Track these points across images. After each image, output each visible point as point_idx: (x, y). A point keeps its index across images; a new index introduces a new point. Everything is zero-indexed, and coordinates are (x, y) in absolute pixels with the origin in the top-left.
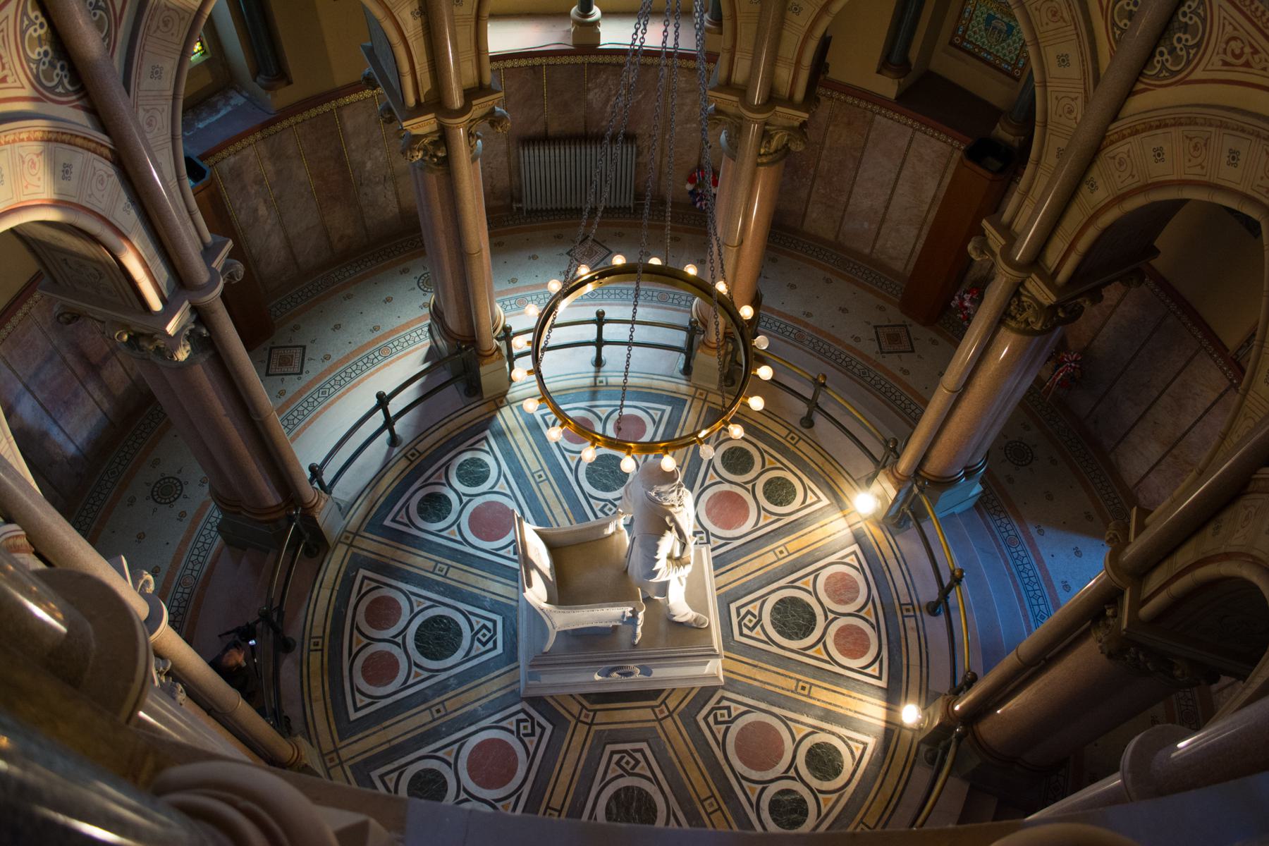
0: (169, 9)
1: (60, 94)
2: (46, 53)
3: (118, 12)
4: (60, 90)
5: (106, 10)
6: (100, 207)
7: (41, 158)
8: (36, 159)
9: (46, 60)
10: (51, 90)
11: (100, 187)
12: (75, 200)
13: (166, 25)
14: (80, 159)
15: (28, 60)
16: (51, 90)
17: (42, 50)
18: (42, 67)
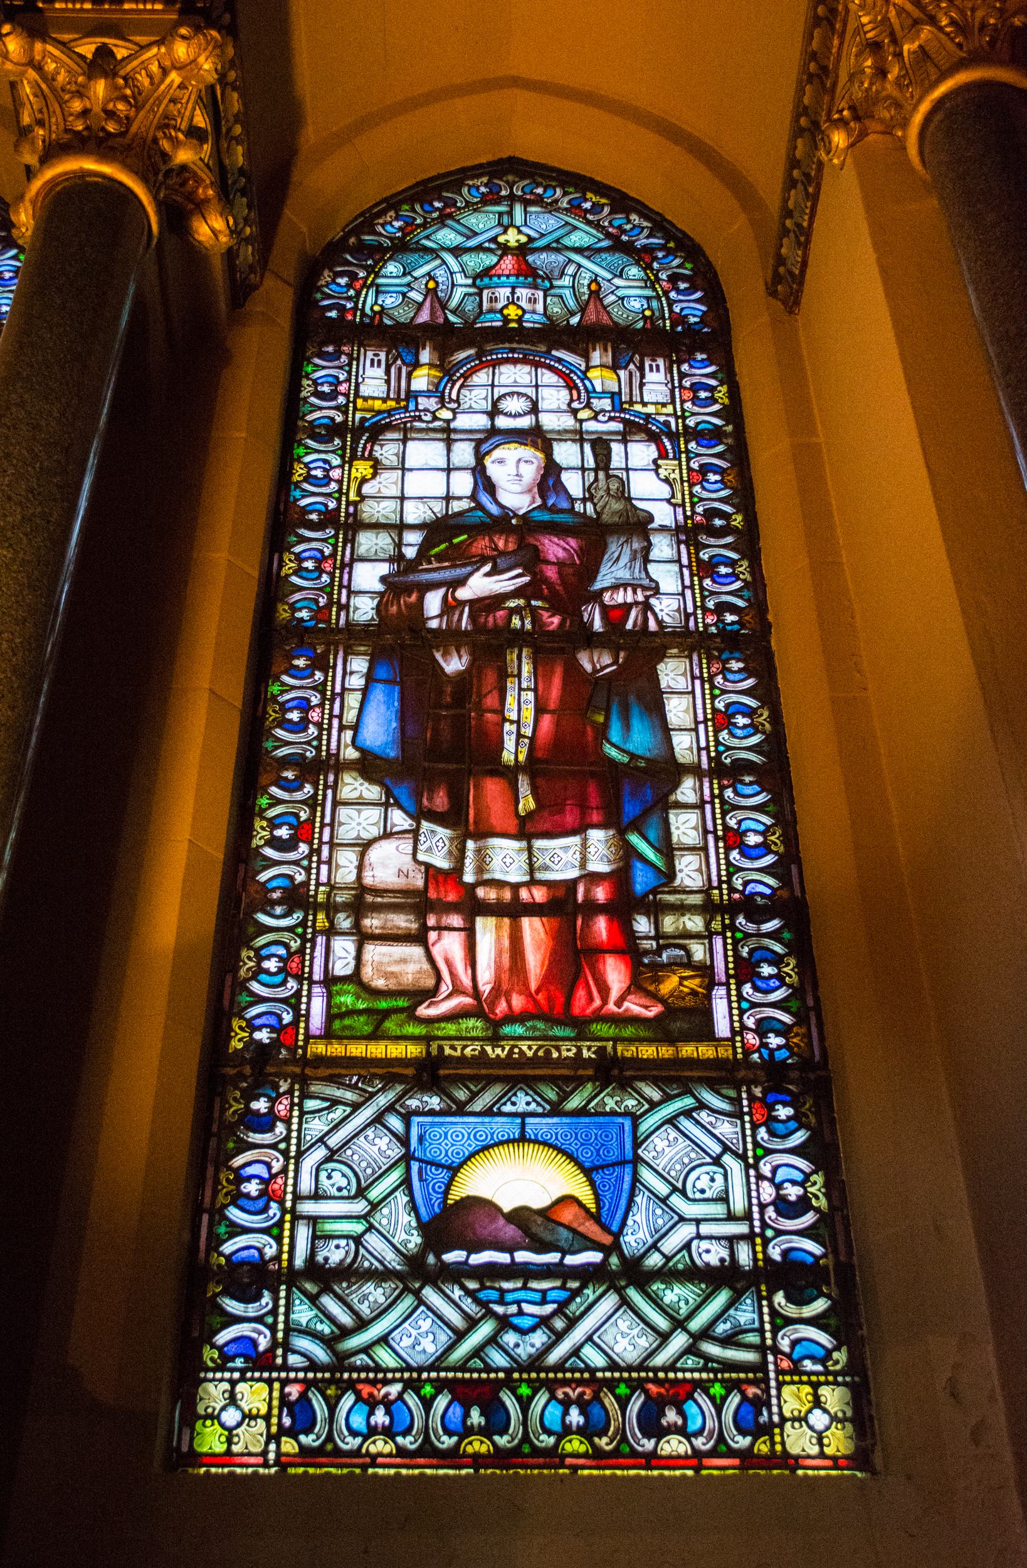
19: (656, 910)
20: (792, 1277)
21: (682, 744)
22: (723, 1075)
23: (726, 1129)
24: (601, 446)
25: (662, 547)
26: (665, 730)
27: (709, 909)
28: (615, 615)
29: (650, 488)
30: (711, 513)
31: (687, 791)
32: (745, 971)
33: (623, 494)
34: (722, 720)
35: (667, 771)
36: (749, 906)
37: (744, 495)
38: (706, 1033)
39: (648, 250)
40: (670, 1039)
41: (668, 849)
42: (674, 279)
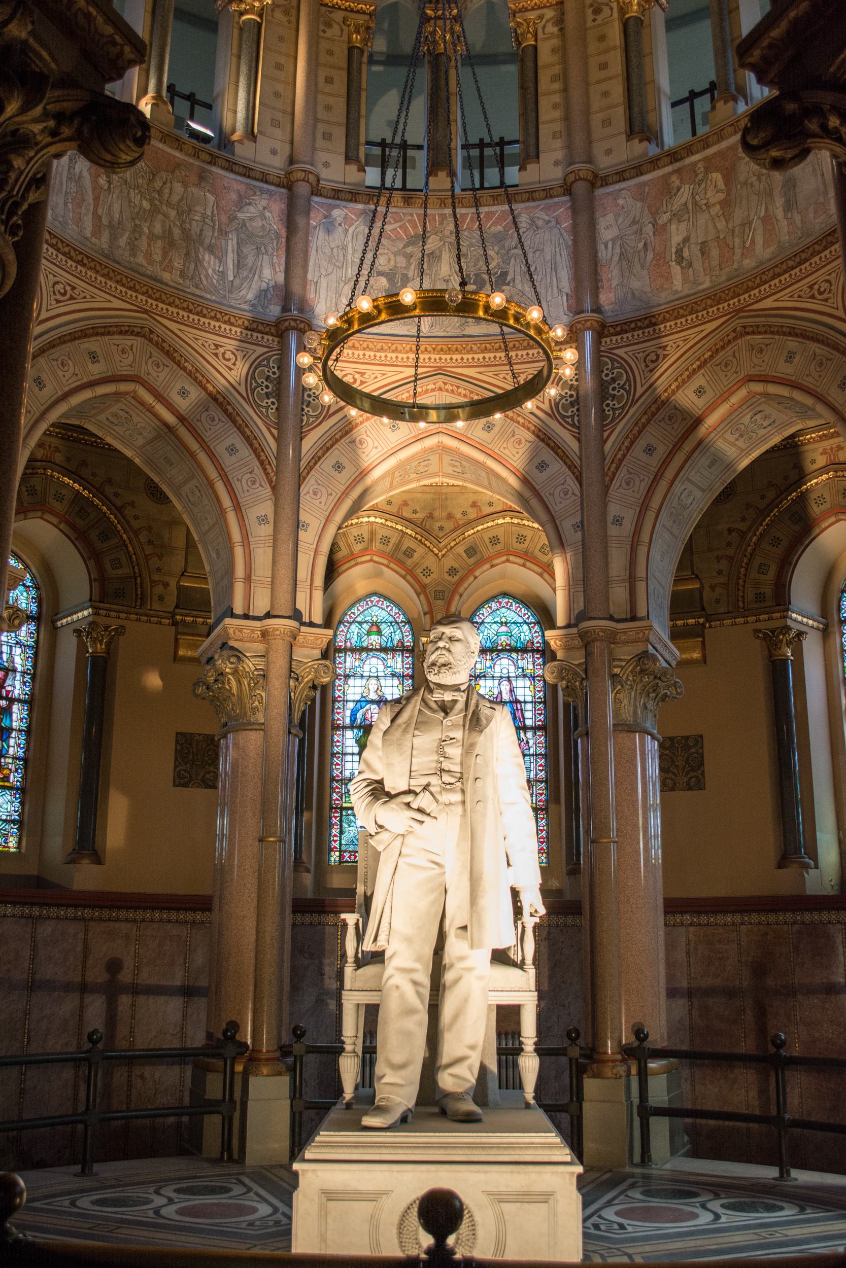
0: (676, 409)
1: (567, 423)
2: (571, 396)
3: (636, 397)
4: (569, 420)
5: (628, 392)
6: (556, 508)
7: (528, 445)
8: (523, 441)
9: (570, 400)
10: (563, 417)
11: (562, 495)
12: (537, 487)
14: (556, 467)
16: (563, 417)
17: (569, 393)
18: (564, 401)
19: (5, 757)
20: (14, 822)
21: (15, 725)
22: (10, 788)
23: (9, 798)
24: (11, 647)
25: (18, 675)
26: (12, 721)
27: (13, 758)
28: (8, 692)
29: (18, 661)
30: (28, 669)
31: (13, 735)
32: (16, 771)
33: (13, 662)
34: (21, 720)
35: (10, 730)
36: (19, 759)
37: (35, 666)
38: (8, 781)
39: (29, 587)
40: (4, 781)
41: (9, 746)
42: (33, 598)
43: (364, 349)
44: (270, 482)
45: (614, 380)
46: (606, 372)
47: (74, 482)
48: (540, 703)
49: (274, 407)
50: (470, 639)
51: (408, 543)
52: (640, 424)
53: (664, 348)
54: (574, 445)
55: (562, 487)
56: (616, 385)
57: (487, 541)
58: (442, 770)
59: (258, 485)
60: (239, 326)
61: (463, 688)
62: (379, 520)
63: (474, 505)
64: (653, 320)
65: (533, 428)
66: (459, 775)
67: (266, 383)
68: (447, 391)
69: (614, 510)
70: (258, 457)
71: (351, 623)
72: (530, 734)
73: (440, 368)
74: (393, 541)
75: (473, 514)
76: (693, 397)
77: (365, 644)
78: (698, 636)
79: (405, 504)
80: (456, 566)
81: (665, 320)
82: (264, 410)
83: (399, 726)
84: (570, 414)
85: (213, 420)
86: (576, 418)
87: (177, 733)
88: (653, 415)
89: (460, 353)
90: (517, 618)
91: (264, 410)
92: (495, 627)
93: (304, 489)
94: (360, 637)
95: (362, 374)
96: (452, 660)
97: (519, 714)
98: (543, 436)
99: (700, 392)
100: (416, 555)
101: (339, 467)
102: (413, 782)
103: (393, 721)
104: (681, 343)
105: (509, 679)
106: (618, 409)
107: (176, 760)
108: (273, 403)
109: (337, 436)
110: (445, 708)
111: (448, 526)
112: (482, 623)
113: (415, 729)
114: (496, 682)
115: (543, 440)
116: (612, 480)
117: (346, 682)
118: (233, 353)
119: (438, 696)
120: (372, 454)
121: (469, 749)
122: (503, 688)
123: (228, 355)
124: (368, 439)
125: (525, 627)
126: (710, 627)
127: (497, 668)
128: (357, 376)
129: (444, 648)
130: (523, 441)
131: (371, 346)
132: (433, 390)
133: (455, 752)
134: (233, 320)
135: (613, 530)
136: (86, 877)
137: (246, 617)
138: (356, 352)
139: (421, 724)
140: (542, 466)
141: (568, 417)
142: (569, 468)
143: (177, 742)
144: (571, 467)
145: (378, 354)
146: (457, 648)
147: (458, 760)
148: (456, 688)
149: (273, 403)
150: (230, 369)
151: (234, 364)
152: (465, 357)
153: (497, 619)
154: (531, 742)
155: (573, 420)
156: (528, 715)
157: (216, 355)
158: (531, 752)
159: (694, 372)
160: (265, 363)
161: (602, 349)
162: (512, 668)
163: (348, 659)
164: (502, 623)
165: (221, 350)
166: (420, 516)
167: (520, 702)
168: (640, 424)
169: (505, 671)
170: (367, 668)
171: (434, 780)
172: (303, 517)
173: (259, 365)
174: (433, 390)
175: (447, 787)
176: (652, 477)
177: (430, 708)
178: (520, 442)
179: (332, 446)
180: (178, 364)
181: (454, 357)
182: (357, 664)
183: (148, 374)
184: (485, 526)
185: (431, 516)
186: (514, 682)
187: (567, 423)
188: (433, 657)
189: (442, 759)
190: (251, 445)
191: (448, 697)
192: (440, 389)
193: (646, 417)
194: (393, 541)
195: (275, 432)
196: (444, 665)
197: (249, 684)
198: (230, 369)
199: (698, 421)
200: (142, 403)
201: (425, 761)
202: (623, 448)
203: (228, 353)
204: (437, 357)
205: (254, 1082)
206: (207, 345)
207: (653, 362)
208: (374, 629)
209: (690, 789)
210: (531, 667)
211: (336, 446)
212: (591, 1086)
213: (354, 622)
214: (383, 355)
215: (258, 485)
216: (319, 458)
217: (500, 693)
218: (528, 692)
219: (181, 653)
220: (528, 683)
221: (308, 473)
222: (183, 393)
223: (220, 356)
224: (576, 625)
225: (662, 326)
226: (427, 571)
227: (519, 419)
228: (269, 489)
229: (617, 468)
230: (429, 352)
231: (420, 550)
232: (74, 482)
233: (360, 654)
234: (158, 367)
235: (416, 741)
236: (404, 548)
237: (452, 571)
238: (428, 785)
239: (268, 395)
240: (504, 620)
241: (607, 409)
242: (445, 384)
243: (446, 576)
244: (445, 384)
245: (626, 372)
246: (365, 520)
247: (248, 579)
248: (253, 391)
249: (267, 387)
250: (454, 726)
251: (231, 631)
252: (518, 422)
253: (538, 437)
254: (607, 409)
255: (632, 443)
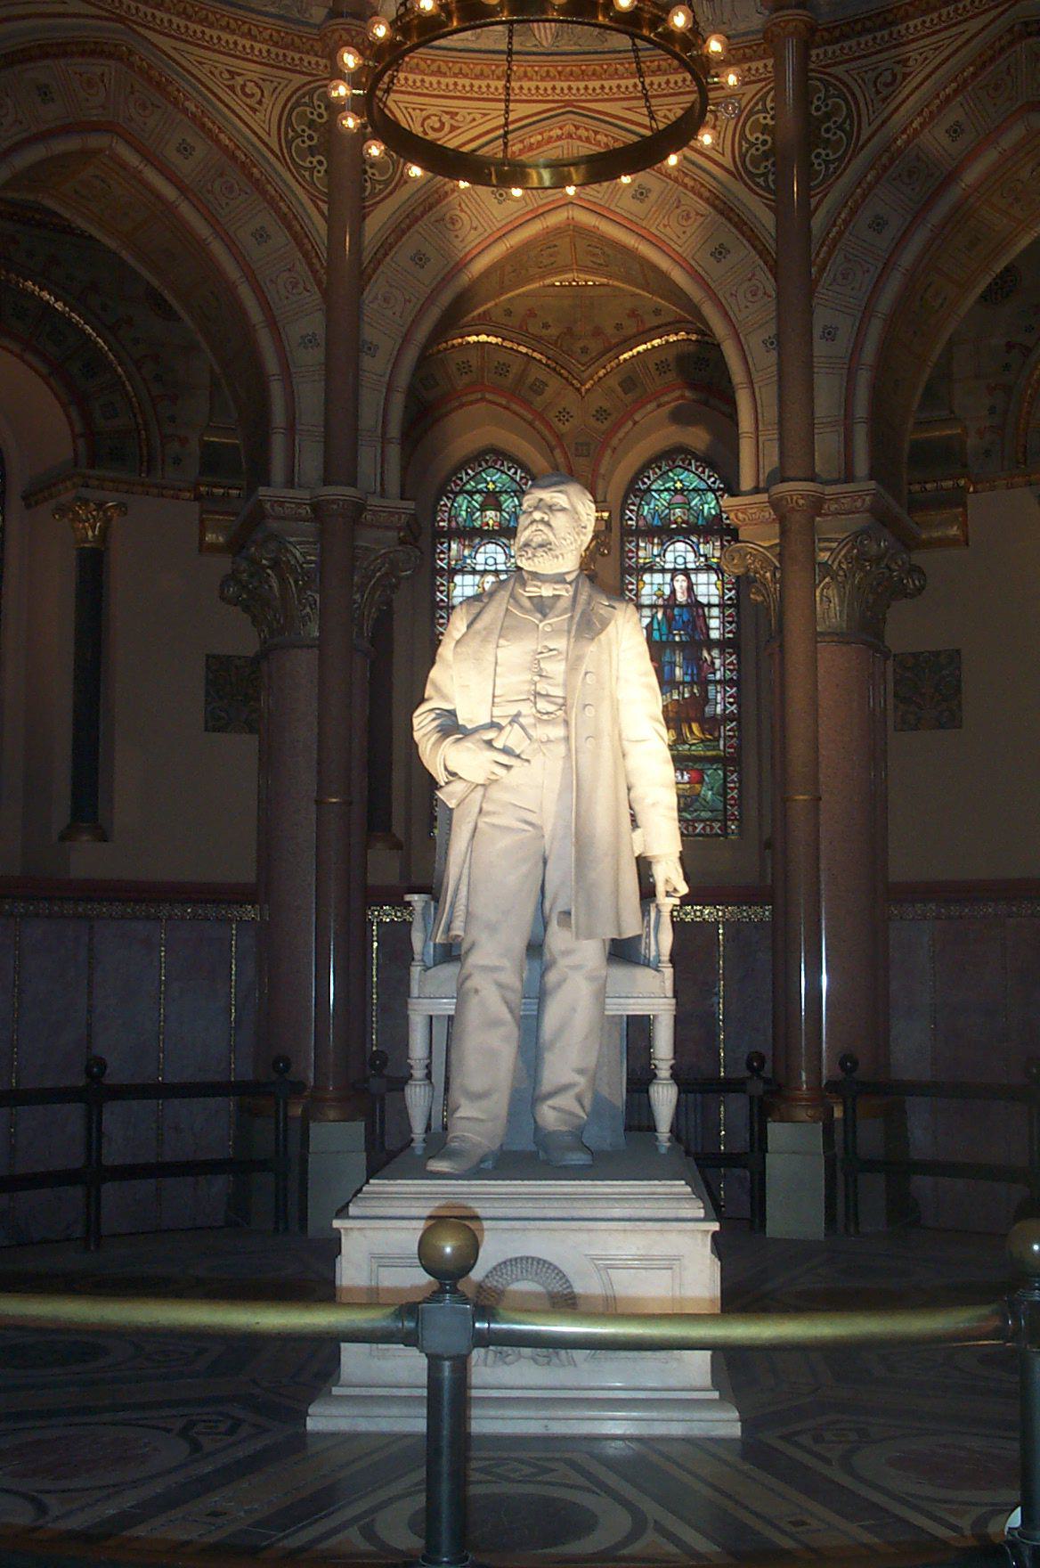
1: (758, 184)
2: (765, 142)
4: (761, 181)
5: (849, 135)
8: (693, 214)
13: (910, 176)
14: (743, 253)
15: (743, 136)
17: (762, 138)
18: (753, 150)
43: (455, 75)
44: (319, 283)
45: (828, 116)
46: (816, 103)
47: (41, 289)
48: (730, 606)
49: (322, 169)
50: (580, 508)
51: (536, 373)
52: (864, 185)
53: (904, 62)
54: (767, 219)
55: (746, 285)
56: (830, 124)
57: (652, 367)
58: (537, 694)
59: (301, 286)
60: (264, 42)
61: (569, 578)
62: (492, 339)
63: (633, 314)
64: (890, 17)
65: (707, 194)
66: (560, 701)
67: (308, 132)
68: (580, 138)
69: (822, 318)
70: (300, 245)
71: (457, 494)
72: (715, 653)
73: (568, 103)
74: (515, 370)
75: (631, 328)
76: (945, 140)
77: (478, 524)
78: (958, 506)
79: (532, 313)
80: (606, 405)
81: (907, 17)
82: (307, 174)
83: (478, 633)
84: (762, 170)
85: (231, 189)
86: (771, 178)
87: (208, 656)
88: (885, 168)
89: (600, 78)
90: (696, 483)
91: (307, 174)
92: (665, 495)
93: (368, 295)
94: (470, 514)
95: (453, 115)
96: (552, 538)
97: (700, 623)
98: (721, 206)
99: (955, 131)
100: (549, 391)
101: (420, 259)
102: (497, 712)
103: (469, 627)
104: (930, 54)
105: (686, 572)
106: (833, 162)
107: (207, 694)
108: (320, 163)
109: (417, 213)
110: (542, 607)
111: (595, 346)
112: (649, 490)
113: (500, 636)
114: (668, 576)
115: (722, 213)
116: (822, 270)
117: (451, 580)
118: (257, 85)
119: (532, 590)
120: (470, 238)
121: (574, 664)
122: (677, 585)
123: (250, 88)
124: (462, 215)
125: (710, 496)
126: (975, 492)
127: (669, 556)
128: (445, 118)
129: (542, 521)
130: (693, 214)
131: (465, 70)
132: (559, 138)
133: (556, 668)
134: (255, 31)
135: (820, 348)
136: (88, 860)
137: (290, 483)
138: (444, 81)
139: (506, 630)
140: (720, 253)
141: (759, 176)
142: (760, 254)
143: (208, 667)
144: (763, 253)
145: (476, 83)
146: (559, 521)
147: (560, 679)
148: (559, 579)
149: (320, 163)
150: (255, 111)
151: (260, 102)
152: (607, 84)
153: (669, 485)
154: (717, 662)
155: (766, 181)
156: (714, 623)
157: (232, 88)
158: (718, 676)
159: (948, 99)
160: (306, 99)
161: (812, 66)
162: (691, 557)
163: (454, 546)
164: (676, 490)
165: (240, 80)
166: (553, 332)
167: (702, 605)
168: (864, 185)
169: (680, 560)
170: (480, 558)
171: (526, 709)
172: (369, 334)
173: (297, 104)
174: (559, 138)
175: (542, 718)
176: (881, 265)
177: (521, 607)
178: (688, 217)
179: (409, 228)
180: (175, 103)
181: (591, 84)
182: (466, 553)
183: (131, 119)
184: (649, 345)
185: (569, 331)
186: (693, 577)
187: (758, 184)
188: (527, 533)
189: (537, 678)
190: (289, 228)
191: (547, 591)
192: (570, 136)
193: (873, 173)
194: (514, 370)
195: (325, 207)
196: (541, 546)
197: (296, 582)
198: (255, 111)
199: (952, 177)
200: (124, 166)
201: (514, 681)
202: (839, 221)
203: (250, 84)
204: (565, 85)
205: (314, 1127)
206: (217, 72)
207: (887, 85)
208: (491, 500)
209: (941, 726)
210: (717, 554)
211: (416, 227)
212: (777, 1132)
213: (462, 492)
214: (484, 83)
215: (301, 286)
216: (391, 246)
217: (673, 591)
218: (713, 590)
219: (210, 537)
220: (714, 577)
221: (374, 271)
222: (185, 149)
223: (238, 89)
224: (766, 490)
225: (902, 28)
226: (564, 415)
227: (687, 180)
228: (318, 296)
229: (830, 253)
230: (553, 79)
231: (554, 383)
232: (41, 289)
233: (471, 540)
234: (145, 108)
235: (500, 653)
236: (530, 380)
237: (601, 414)
238: (518, 715)
239: (312, 151)
240: (679, 485)
241: (816, 161)
242: (577, 128)
243: (592, 421)
244: (577, 128)
245: (847, 103)
246: (473, 339)
247: (291, 429)
248: (289, 143)
249: (311, 138)
250: (556, 632)
251: (268, 506)
252: (685, 186)
253: (715, 207)
254: (816, 161)
255: (853, 212)
